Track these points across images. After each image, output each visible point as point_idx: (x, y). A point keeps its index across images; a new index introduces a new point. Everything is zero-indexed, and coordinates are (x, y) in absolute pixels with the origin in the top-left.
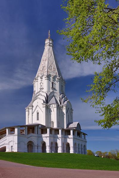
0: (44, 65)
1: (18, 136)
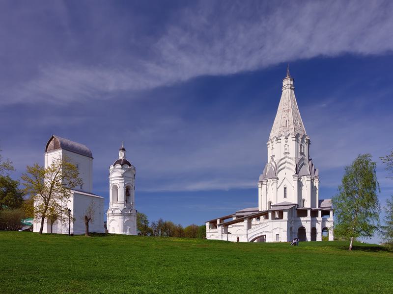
0: (287, 119)
1: (288, 221)
